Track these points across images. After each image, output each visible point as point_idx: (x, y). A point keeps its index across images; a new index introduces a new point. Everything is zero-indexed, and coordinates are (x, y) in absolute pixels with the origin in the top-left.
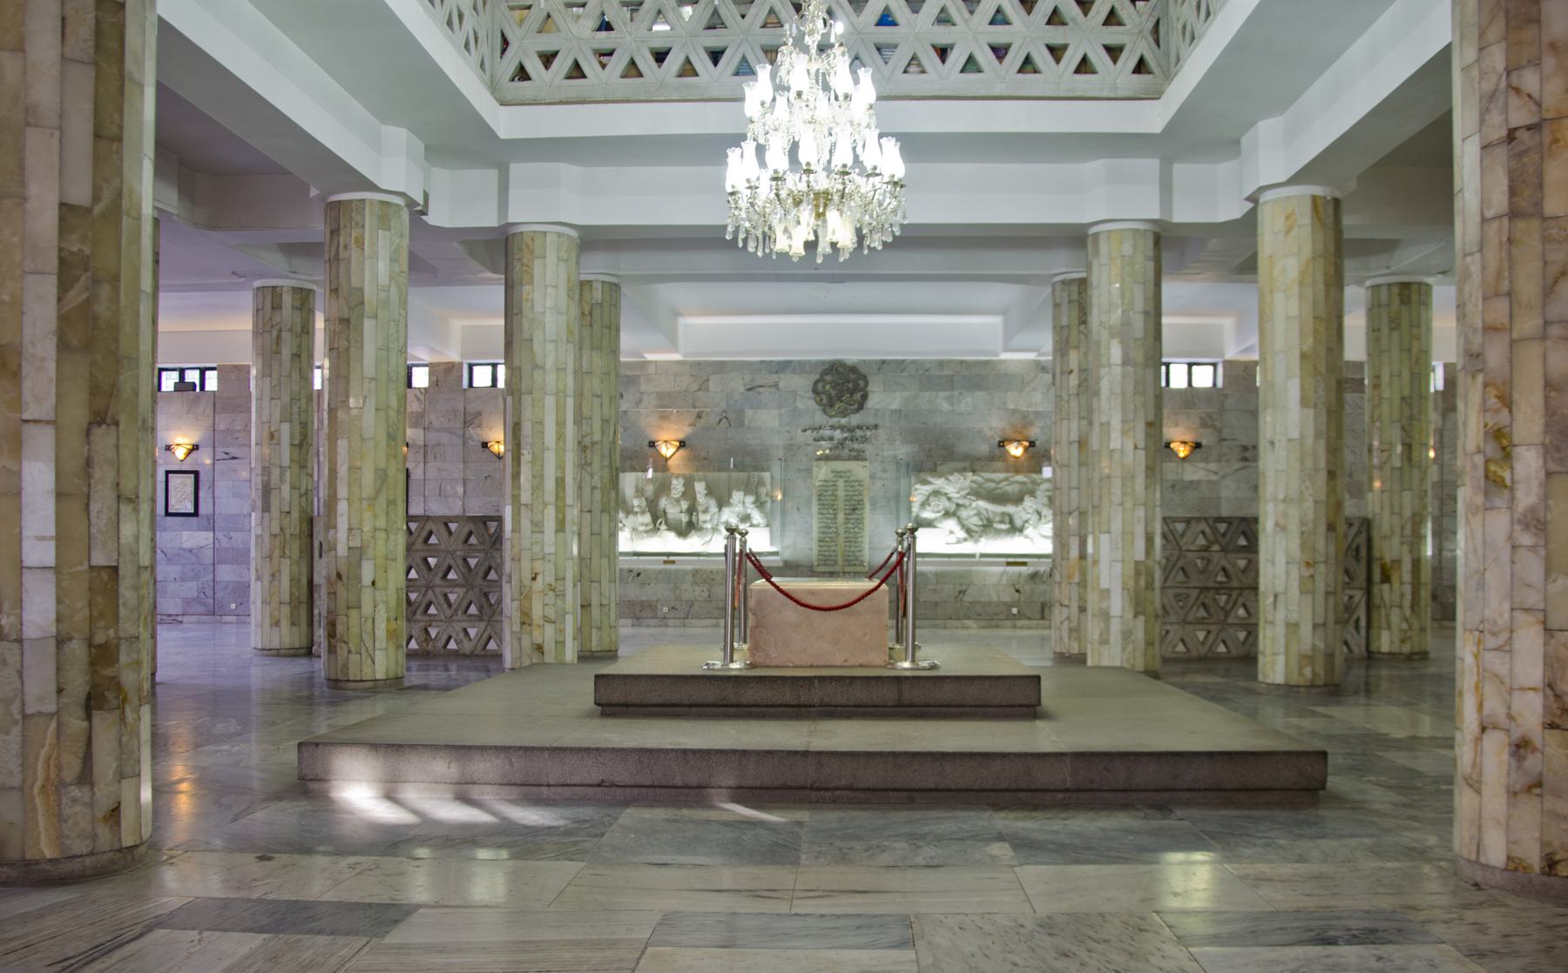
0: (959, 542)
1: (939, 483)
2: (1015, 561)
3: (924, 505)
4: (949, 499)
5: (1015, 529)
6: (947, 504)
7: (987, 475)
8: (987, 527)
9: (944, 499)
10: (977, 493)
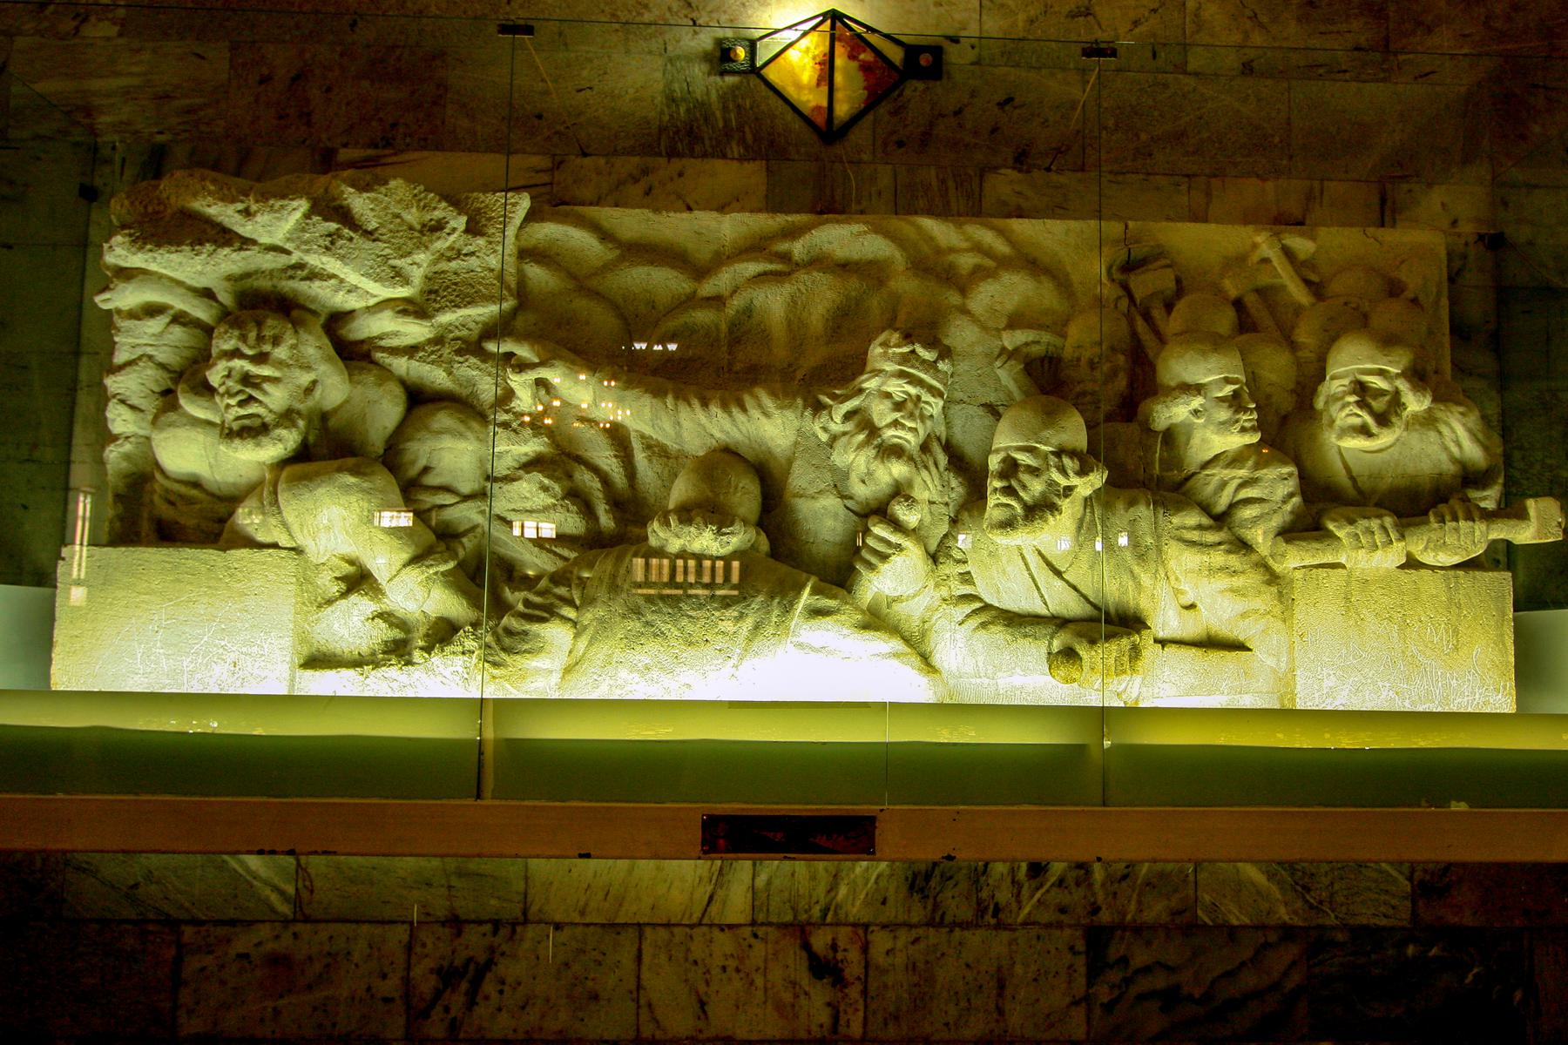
0: (398, 650)
1: (278, 225)
2: (778, 807)
3: (187, 377)
4: (355, 355)
5: (794, 561)
6: (334, 388)
7: (631, 222)
8: (612, 532)
9: (313, 346)
10: (558, 323)
